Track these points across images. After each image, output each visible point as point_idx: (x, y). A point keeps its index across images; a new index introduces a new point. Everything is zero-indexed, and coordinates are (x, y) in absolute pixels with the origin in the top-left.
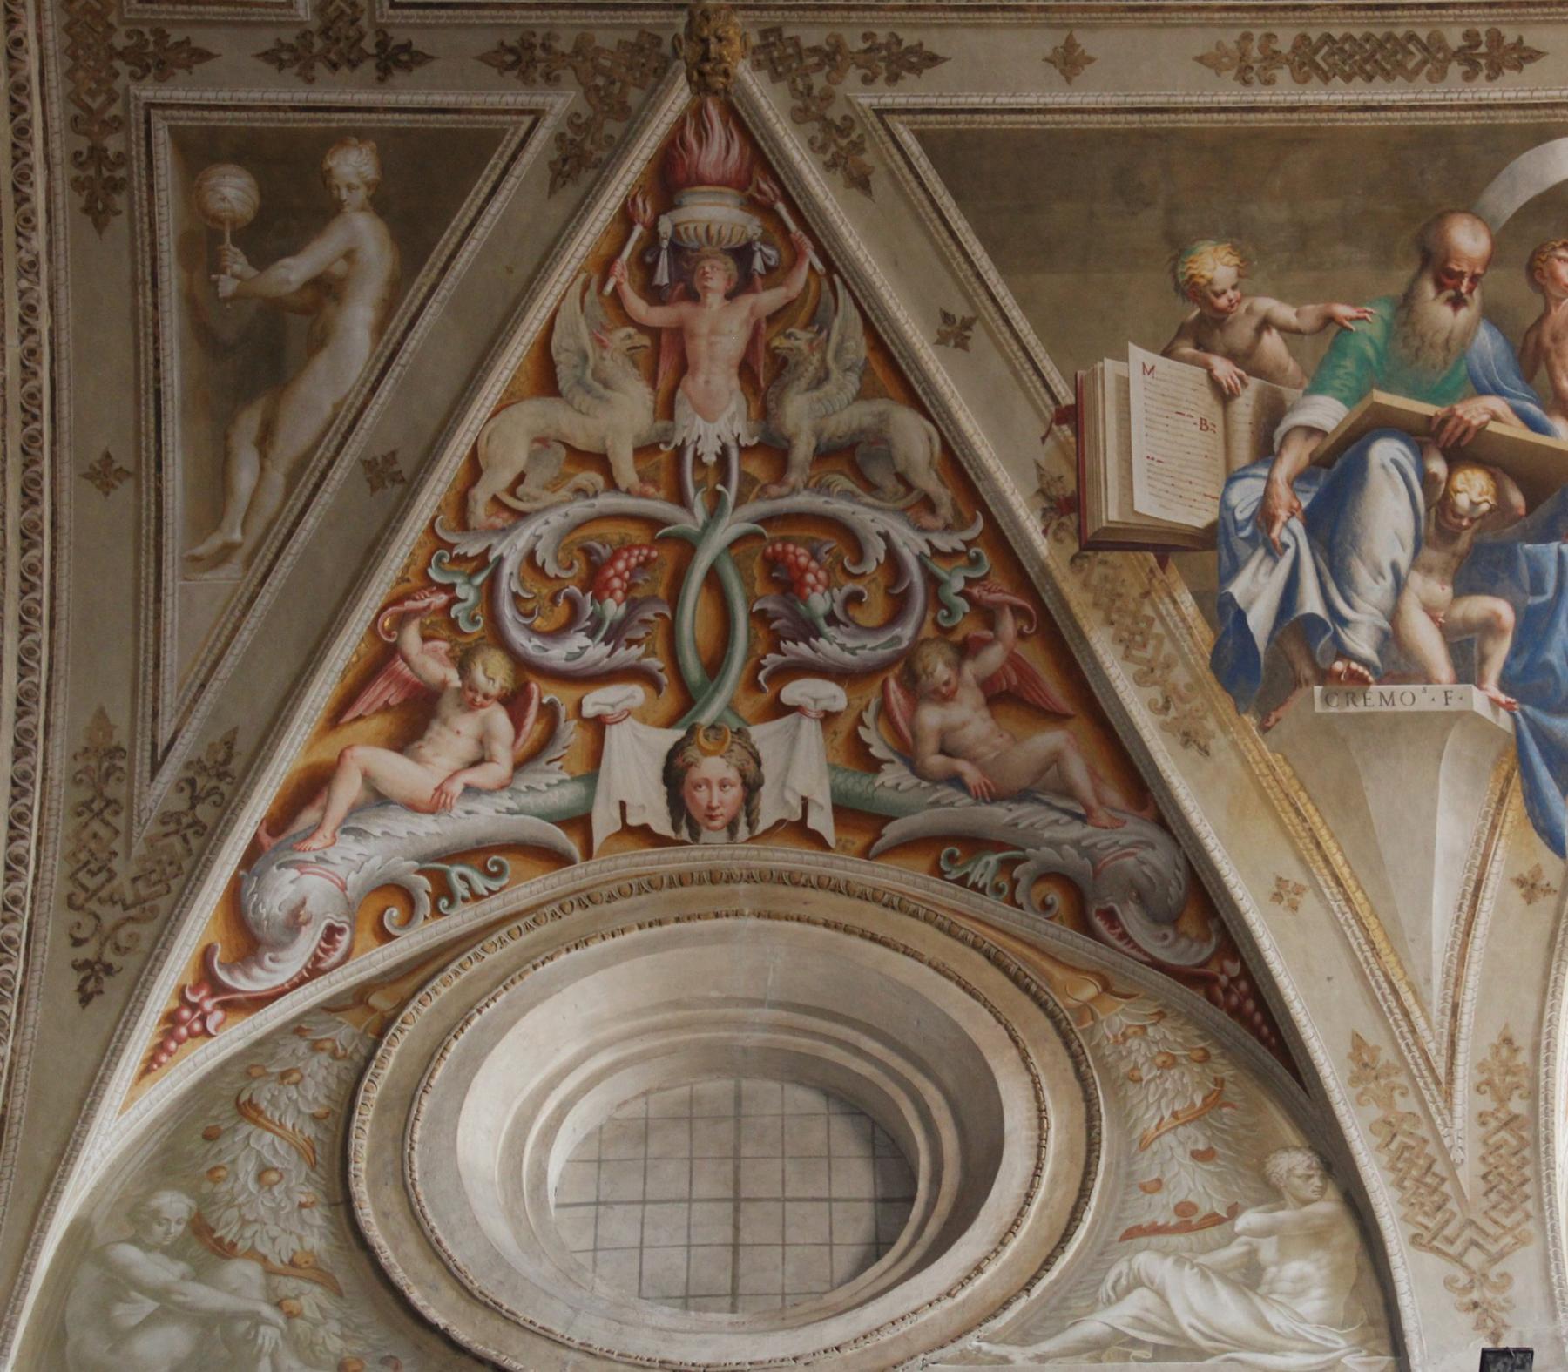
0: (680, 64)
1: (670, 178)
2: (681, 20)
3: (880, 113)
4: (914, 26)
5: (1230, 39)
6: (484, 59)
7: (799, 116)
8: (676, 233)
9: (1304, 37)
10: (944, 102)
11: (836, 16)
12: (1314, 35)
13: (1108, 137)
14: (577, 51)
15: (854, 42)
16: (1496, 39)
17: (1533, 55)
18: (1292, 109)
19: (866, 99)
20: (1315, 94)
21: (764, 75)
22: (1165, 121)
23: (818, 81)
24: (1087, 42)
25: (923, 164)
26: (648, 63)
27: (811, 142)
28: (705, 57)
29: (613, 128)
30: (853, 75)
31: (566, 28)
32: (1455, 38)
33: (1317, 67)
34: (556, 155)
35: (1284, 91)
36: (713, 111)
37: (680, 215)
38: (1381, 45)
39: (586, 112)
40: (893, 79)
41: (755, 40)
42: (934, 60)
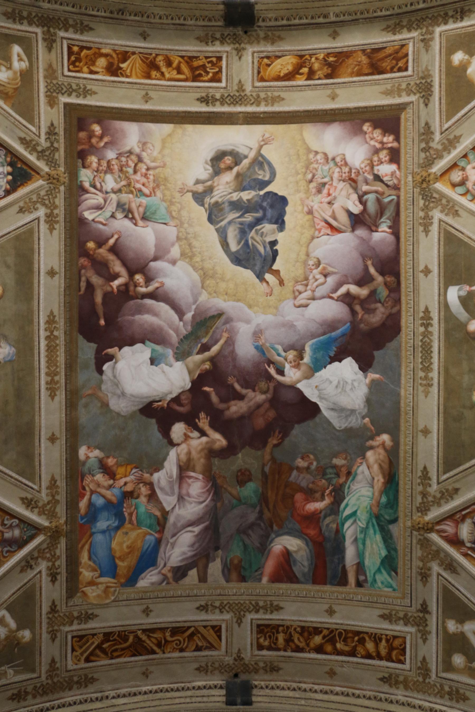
0: (426, 535)
1: (456, 541)
2: (415, 533)
3: (438, 483)
4: (416, 472)
5: (421, 389)
6: (424, 586)
7: (439, 505)
8: (470, 542)
9: (421, 369)
10: (436, 466)
11: (414, 492)
12: (420, 366)
13: (445, 423)
14: (422, 561)
15: (420, 488)
16: (422, 318)
17: (427, 308)
18: (439, 373)
19: (435, 486)
20: (435, 366)
21: (428, 513)
22: (441, 407)
23: (430, 499)
24: (421, 427)
25: (452, 473)
26: (425, 543)
27: (446, 503)
28: (423, 528)
29: (442, 555)
30: (429, 489)
31: (417, 563)
32: (422, 329)
33: (429, 366)
34: (449, 571)
35: (434, 374)
36: (438, 527)
37: (466, 540)
38: (423, 349)
39: (438, 561)
40: (430, 479)
41: (419, 514)
42: (425, 468)
